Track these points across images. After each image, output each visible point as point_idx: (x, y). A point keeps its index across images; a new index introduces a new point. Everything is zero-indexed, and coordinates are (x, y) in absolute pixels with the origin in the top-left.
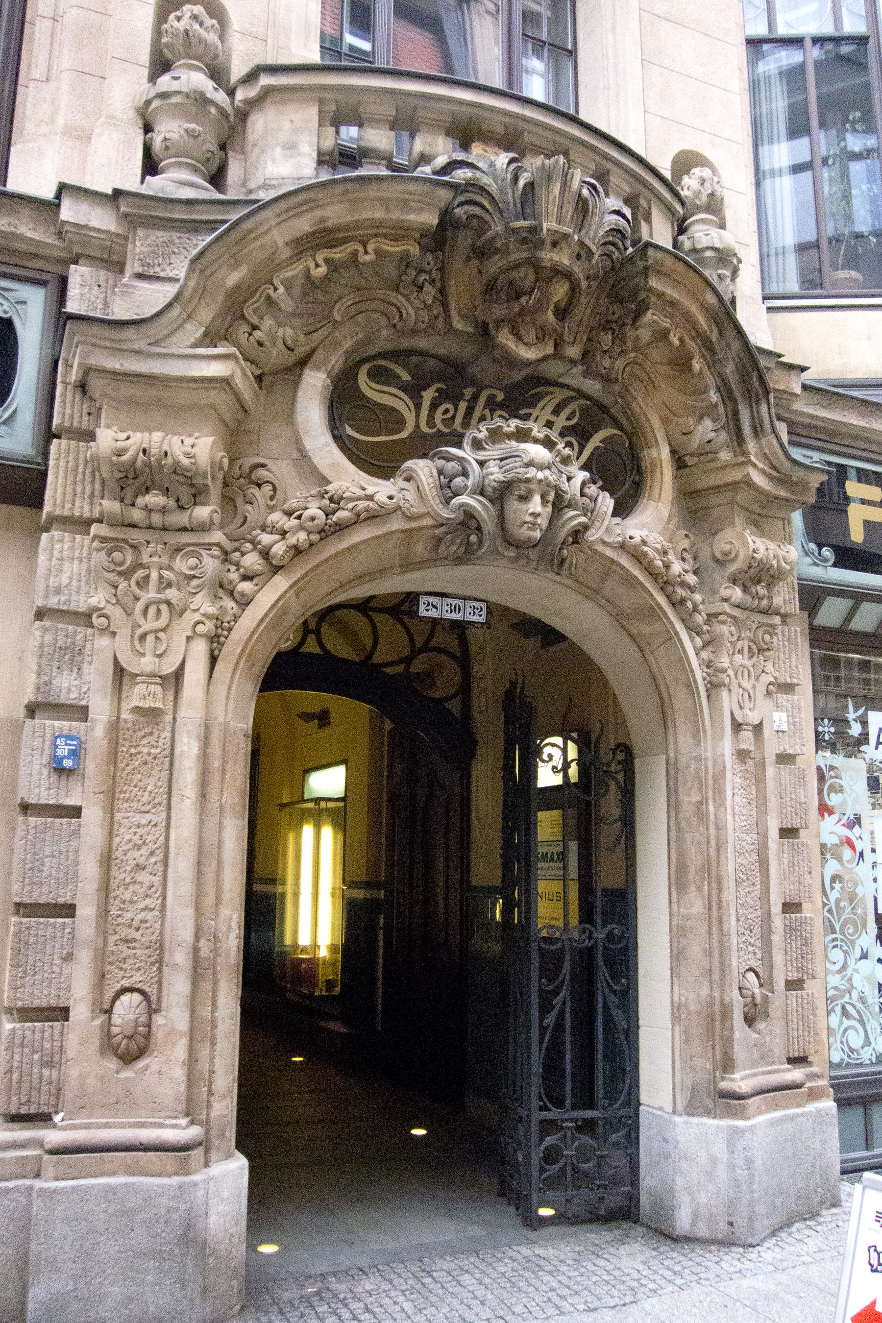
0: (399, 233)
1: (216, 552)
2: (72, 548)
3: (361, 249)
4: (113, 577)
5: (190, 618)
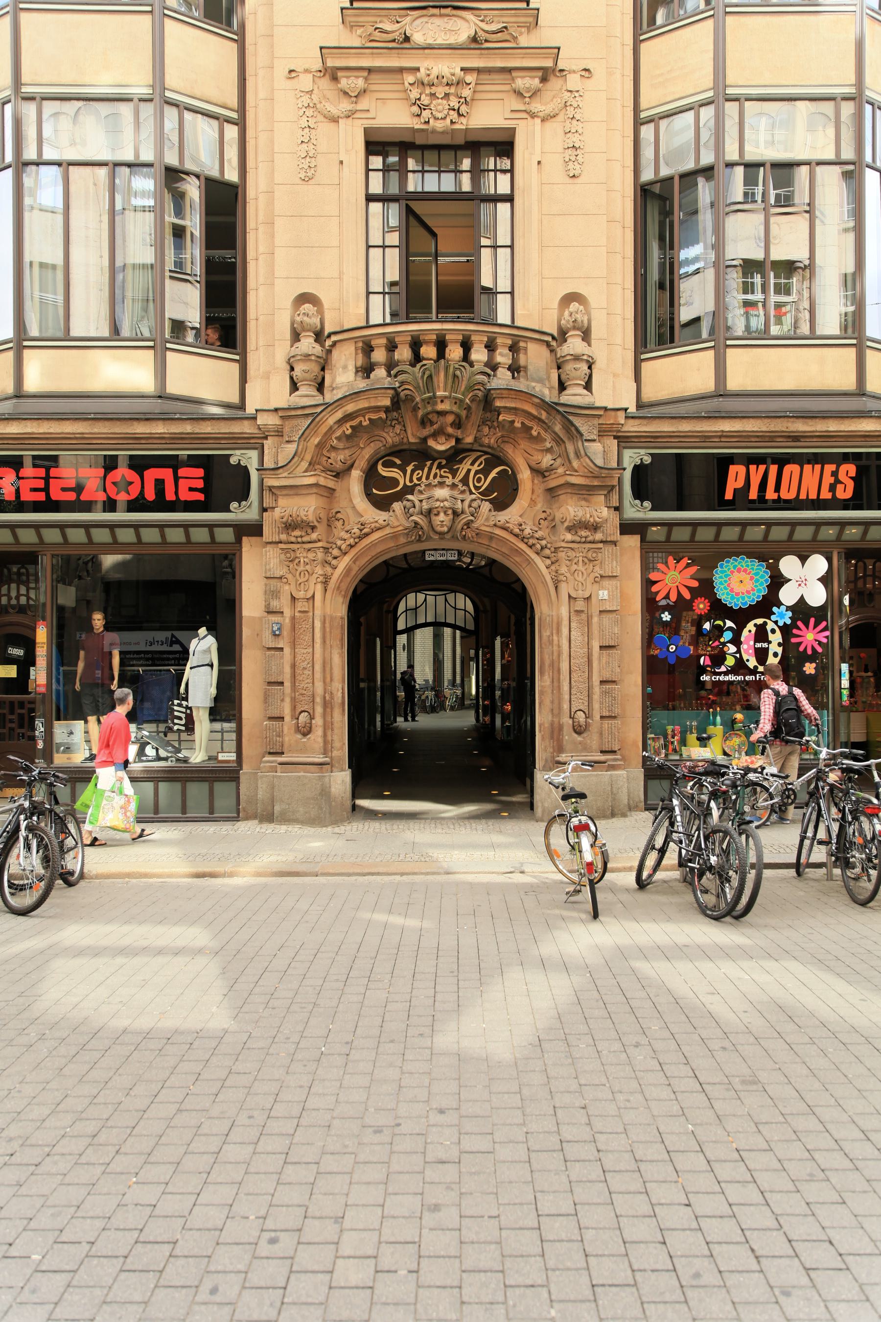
1: (321, 550)
4: (287, 563)
5: (315, 576)
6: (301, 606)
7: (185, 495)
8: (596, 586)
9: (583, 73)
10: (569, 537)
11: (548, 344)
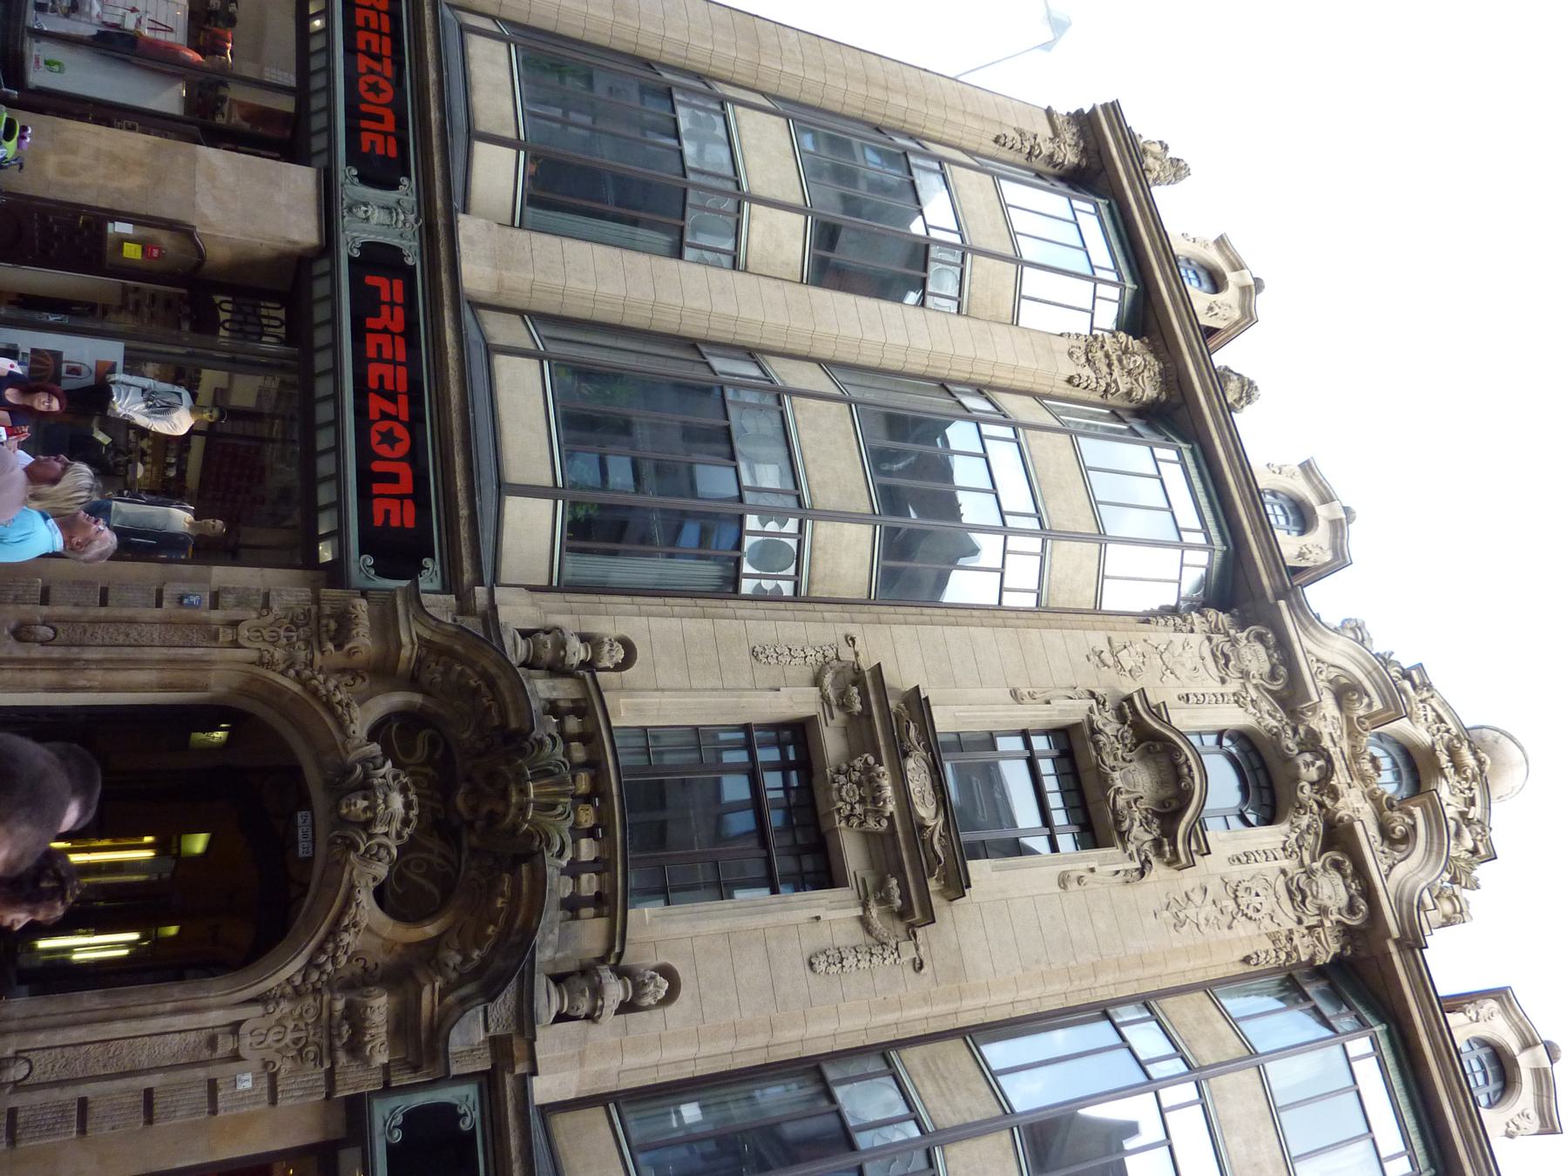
0: (503, 714)
2: (303, 601)
3: (490, 698)
5: (271, 649)
6: (226, 635)
7: (379, 507)
8: (256, 1064)
9: (918, 961)
10: (339, 1005)
11: (611, 948)
